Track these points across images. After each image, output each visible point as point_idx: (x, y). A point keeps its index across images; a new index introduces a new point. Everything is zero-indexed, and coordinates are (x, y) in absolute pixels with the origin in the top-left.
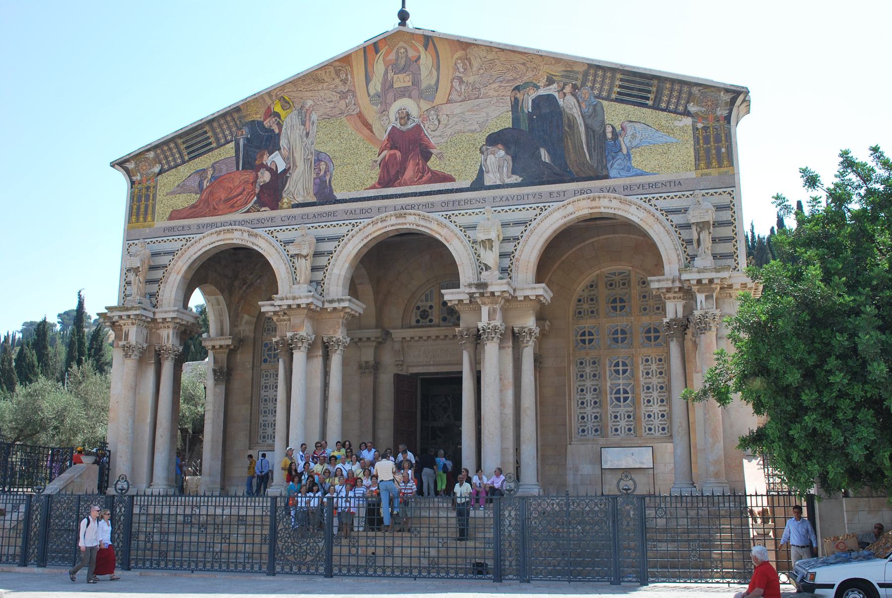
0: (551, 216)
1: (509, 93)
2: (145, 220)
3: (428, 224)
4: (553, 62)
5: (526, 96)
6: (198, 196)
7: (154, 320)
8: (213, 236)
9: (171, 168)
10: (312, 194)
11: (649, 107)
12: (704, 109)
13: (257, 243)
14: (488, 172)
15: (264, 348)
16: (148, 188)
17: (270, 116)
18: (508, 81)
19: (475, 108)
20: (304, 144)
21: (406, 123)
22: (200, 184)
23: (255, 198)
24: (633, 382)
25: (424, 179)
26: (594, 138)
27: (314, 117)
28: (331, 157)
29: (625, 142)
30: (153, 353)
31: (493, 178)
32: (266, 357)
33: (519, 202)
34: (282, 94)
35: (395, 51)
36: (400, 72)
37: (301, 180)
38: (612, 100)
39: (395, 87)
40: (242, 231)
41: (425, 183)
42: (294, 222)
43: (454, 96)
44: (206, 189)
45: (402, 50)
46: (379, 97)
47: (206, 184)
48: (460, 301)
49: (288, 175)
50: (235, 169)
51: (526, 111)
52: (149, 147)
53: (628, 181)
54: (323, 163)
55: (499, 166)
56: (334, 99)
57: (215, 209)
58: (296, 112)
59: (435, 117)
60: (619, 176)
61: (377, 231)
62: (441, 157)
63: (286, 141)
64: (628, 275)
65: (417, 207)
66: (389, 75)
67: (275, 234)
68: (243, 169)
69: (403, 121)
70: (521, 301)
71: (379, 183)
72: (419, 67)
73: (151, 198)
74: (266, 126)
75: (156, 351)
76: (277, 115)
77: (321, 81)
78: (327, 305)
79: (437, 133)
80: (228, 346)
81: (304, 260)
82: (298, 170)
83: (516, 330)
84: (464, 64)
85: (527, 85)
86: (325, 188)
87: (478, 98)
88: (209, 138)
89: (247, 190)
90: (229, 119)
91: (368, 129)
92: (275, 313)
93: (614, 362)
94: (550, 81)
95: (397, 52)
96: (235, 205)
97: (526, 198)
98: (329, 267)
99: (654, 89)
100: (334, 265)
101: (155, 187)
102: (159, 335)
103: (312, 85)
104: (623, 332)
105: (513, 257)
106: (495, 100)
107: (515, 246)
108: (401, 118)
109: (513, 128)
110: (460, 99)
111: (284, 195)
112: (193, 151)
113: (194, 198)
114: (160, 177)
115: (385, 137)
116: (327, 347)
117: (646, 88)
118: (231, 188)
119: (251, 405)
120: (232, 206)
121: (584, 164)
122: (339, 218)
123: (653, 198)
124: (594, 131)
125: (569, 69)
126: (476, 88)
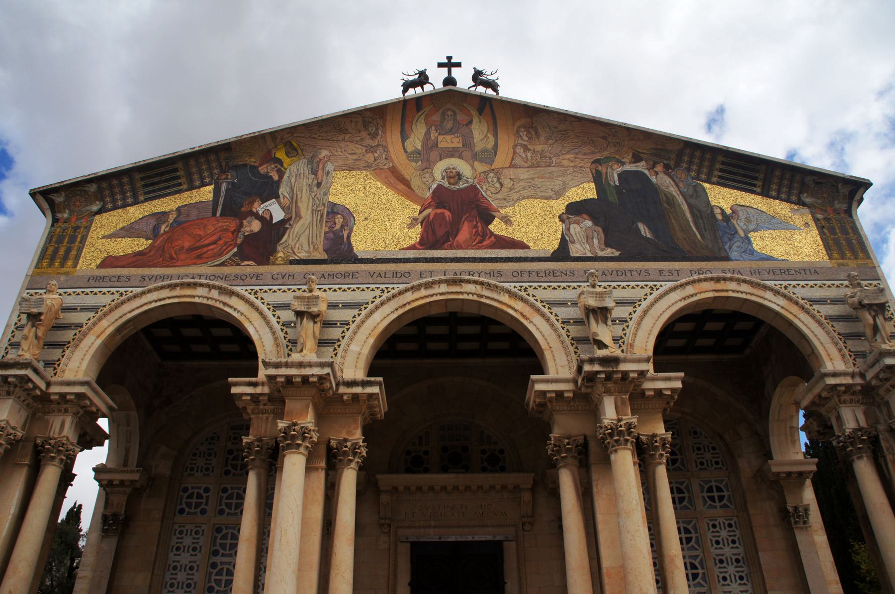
1: (589, 165)
2: (62, 265)
3: (495, 296)
5: (609, 170)
6: (150, 242)
7: (45, 398)
8: (162, 291)
9: (115, 208)
10: (321, 247)
11: (758, 194)
12: (820, 201)
13: (231, 304)
14: (573, 242)
15: (181, 493)
16: (76, 229)
19: (547, 176)
20: (313, 194)
21: (456, 183)
22: (156, 229)
23: (236, 250)
24: (701, 555)
25: (485, 243)
27: (330, 167)
28: (351, 210)
29: (739, 225)
30: (30, 447)
31: (581, 248)
32: (184, 506)
33: (622, 278)
35: (441, 111)
37: (307, 233)
39: (440, 146)
40: (210, 287)
41: (488, 247)
42: (291, 281)
46: (419, 154)
48: (560, 394)
50: (210, 214)
51: (612, 184)
52: (94, 176)
53: (755, 265)
54: (339, 216)
55: (587, 237)
56: (358, 151)
57: (172, 258)
59: (495, 180)
60: (741, 259)
61: (417, 300)
62: (507, 220)
63: (288, 190)
66: (432, 135)
67: (259, 295)
68: (222, 215)
69: (452, 181)
70: (649, 396)
72: (471, 131)
73: (79, 240)
74: (262, 172)
75: (36, 446)
76: (280, 162)
78: (343, 390)
79: (499, 196)
80: (132, 482)
81: (311, 324)
82: (301, 222)
84: (529, 133)
87: (549, 166)
88: (179, 177)
89: (224, 239)
90: (212, 157)
91: (404, 184)
92: (255, 398)
94: (637, 159)
95: (443, 114)
96: (205, 256)
97: (628, 274)
98: (343, 343)
99: (761, 176)
100: (352, 339)
101: (88, 228)
102: (47, 422)
105: (623, 343)
107: (624, 330)
108: (449, 178)
110: (526, 165)
111: (279, 248)
113: (141, 244)
114: (97, 217)
115: (428, 194)
116: (335, 456)
117: (752, 174)
119: (153, 573)
120: (199, 257)
122: (360, 280)
123: (790, 285)
124: (699, 211)
125: (659, 147)
126: (546, 157)
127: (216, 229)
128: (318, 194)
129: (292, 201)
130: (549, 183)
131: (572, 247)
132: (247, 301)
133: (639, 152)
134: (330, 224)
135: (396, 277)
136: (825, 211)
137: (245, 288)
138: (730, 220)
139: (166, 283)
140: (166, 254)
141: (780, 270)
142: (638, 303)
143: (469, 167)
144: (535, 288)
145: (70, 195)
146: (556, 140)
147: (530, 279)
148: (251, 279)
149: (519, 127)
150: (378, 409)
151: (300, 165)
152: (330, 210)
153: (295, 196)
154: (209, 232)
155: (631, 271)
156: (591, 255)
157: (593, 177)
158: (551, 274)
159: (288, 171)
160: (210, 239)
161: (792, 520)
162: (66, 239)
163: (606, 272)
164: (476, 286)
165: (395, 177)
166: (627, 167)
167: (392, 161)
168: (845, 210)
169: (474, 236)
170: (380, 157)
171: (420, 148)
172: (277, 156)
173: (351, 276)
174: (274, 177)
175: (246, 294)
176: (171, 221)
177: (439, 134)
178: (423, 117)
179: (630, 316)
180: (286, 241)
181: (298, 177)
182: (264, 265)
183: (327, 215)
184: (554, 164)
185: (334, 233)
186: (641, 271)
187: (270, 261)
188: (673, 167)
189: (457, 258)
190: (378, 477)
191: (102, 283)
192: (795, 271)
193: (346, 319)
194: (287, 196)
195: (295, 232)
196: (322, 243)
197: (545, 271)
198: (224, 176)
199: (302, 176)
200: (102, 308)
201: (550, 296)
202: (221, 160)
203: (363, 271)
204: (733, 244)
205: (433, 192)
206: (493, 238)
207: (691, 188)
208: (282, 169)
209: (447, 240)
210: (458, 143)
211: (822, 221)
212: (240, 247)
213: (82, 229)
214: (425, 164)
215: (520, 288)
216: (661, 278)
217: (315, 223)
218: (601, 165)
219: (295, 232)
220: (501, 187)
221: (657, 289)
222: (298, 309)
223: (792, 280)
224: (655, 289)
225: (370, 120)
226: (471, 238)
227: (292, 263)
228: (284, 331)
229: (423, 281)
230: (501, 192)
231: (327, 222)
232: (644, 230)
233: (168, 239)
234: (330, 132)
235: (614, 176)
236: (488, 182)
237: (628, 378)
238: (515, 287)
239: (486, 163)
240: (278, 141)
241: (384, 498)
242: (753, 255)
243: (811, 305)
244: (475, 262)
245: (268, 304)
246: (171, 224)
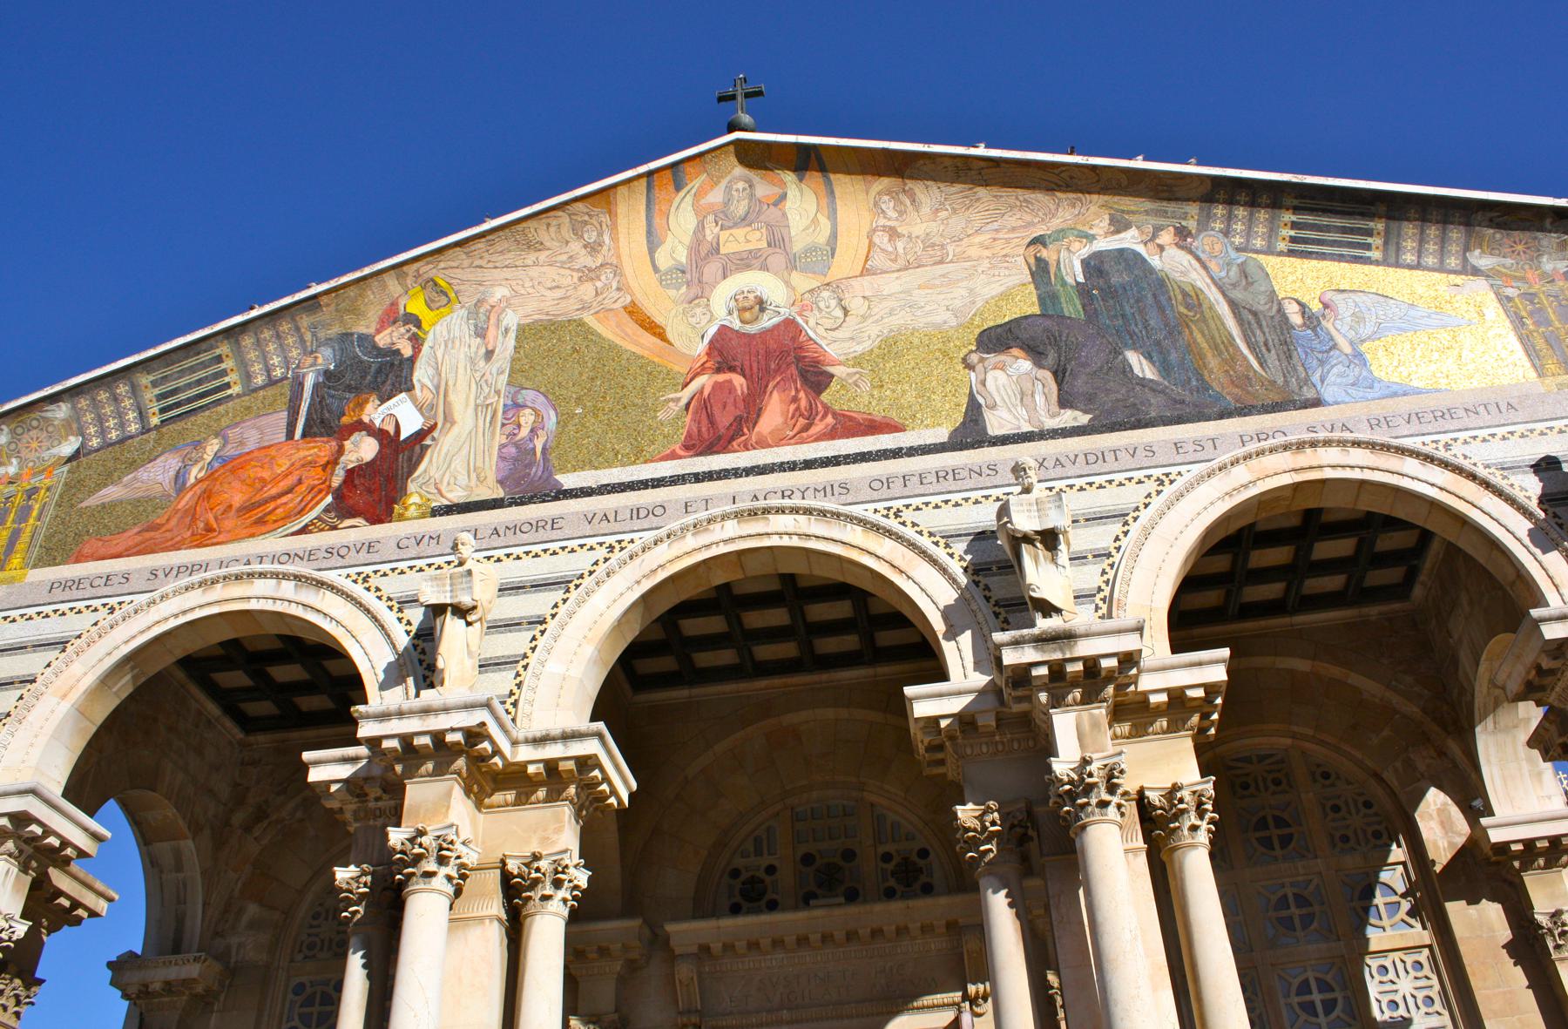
0: (1189, 497)
1: (1021, 250)
4: (1125, 183)
5: (1064, 254)
10: (491, 476)
11: (1377, 263)
14: (993, 407)
17: (394, 322)
18: (1014, 229)
20: (478, 375)
23: (329, 499)
25: (815, 430)
26: (1260, 326)
29: (1340, 329)
34: (431, 275)
36: (735, 225)
37: (464, 452)
38: (1280, 254)
41: (819, 438)
43: (878, 260)
44: (194, 485)
45: (741, 185)
47: (195, 473)
49: (428, 442)
50: (282, 437)
51: (1070, 281)
53: (1378, 409)
54: (528, 411)
55: (1022, 394)
57: (209, 529)
58: (463, 312)
63: (431, 371)
64: (1282, 761)
65: (798, 494)
66: (708, 232)
68: (304, 435)
69: (747, 315)
71: (687, 447)
72: (784, 215)
77: (538, 246)
82: (455, 430)
83: (1154, 797)
85: (1060, 234)
86: (530, 465)
87: (941, 262)
88: (224, 373)
93: (1296, 982)
95: (729, 188)
97: (1110, 457)
103: (510, 255)
104: (1301, 901)
106: (986, 264)
108: (742, 310)
109: (1042, 315)
110: (896, 266)
111: (412, 486)
112: (178, 405)
115: (701, 348)
118: (262, 480)
120: (261, 521)
121: (1248, 378)
122: (567, 532)
123: (1455, 440)
124: (1255, 314)
126: (933, 245)
127: (293, 464)
128: (488, 373)
129: (438, 393)
130: (943, 296)
131: (990, 416)
132: (348, 597)
133: (1123, 212)
134: (509, 429)
135: (638, 518)
136: (1523, 279)
137: (345, 572)
138: (1319, 323)
139: (196, 578)
140: (198, 522)
141: (1433, 412)
142: (1133, 514)
143: (781, 285)
144: (918, 509)
145: (19, 431)
146: (954, 211)
147: (906, 492)
148: (358, 552)
149: (879, 193)
150: (604, 787)
151: (454, 321)
152: (509, 402)
153: (443, 384)
154: (279, 472)
155: (1114, 451)
156: (1031, 429)
157: (1032, 274)
158: (950, 477)
159: (430, 337)
160: (282, 484)
161: (1551, 945)
162: (12, 515)
163: (1063, 460)
164: (797, 517)
165: (636, 322)
166: (1101, 244)
167: (629, 291)
168: (1564, 273)
169: (792, 418)
170: (607, 287)
171: (684, 260)
172: (408, 310)
173: (549, 527)
174: (403, 352)
175: (348, 585)
176: (209, 459)
177: (721, 230)
178: (689, 198)
179: (1117, 544)
180: (425, 471)
181: (450, 345)
182: (381, 521)
183: (504, 412)
184: (950, 257)
185: (516, 445)
186: (1135, 448)
187: (395, 514)
188: (1193, 231)
189: (758, 467)
190: (671, 928)
191: (75, 592)
192: (1466, 410)
193: (539, 613)
194: (429, 384)
195: (444, 450)
196: (494, 468)
197: (937, 473)
198: (310, 360)
199: (457, 343)
200: (73, 641)
201: (947, 522)
202: (303, 330)
203: (573, 513)
204: (1328, 372)
205: (711, 342)
206: (830, 420)
207: (1234, 271)
208: (419, 333)
209: (739, 432)
210: (760, 240)
211: (1517, 300)
212: (339, 495)
213: (43, 491)
214: (695, 290)
215: (885, 512)
216: (1179, 459)
217: (481, 430)
218: (1045, 245)
219: (444, 450)
220: (846, 315)
221: (1172, 482)
222: (433, 601)
223: (1460, 430)
224: (1167, 482)
225: (586, 218)
226: (785, 422)
227: (435, 512)
228: (419, 649)
229: (690, 519)
230: (844, 325)
231: (503, 425)
232: (1140, 365)
233: (205, 492)
234: (510, 251)
235: (1073, 266)
236: (820, 310)
237: (1099, 672)
238: (876, 511)
239: (814, 273)
240: (409, 281)
241: (684, 971)
242: (1371, 387)
243: (1505, 477)
244: (793, 469)
245: (389, 599)
246: (210, 463)
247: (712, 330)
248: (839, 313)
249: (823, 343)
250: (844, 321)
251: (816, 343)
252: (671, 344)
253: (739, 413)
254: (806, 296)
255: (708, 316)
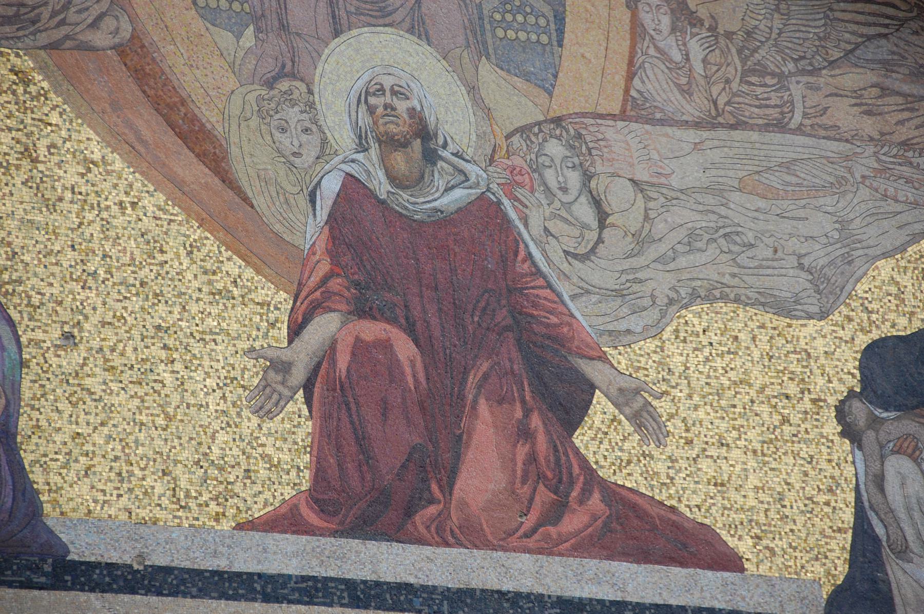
69: (399, 160)
108: (390, 143)
205: (333, 219)
220: (602, 225)
236: (548, 189)
247: (331, 186)
248: (585, 212)
249: (565, 290)
250: (600, 240)
251: (553, 290)
252: (246, 199)
253: (418, 440)
254: (516, 139)
255: (315, 139)
